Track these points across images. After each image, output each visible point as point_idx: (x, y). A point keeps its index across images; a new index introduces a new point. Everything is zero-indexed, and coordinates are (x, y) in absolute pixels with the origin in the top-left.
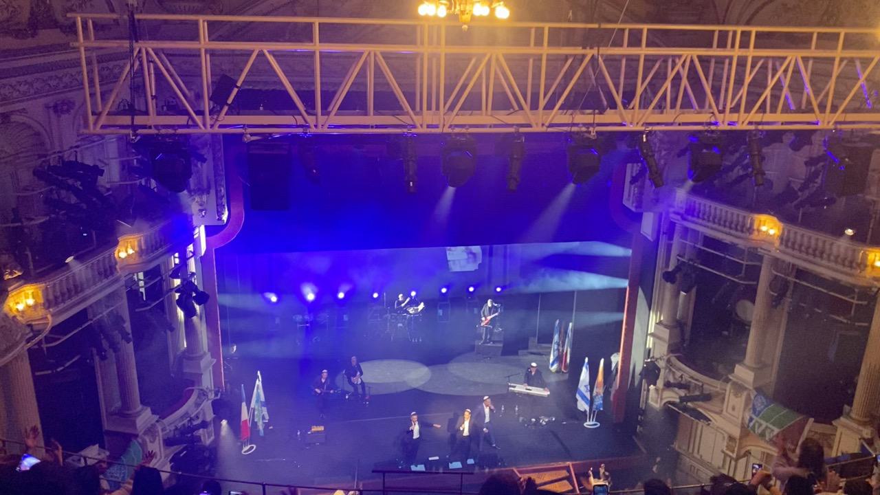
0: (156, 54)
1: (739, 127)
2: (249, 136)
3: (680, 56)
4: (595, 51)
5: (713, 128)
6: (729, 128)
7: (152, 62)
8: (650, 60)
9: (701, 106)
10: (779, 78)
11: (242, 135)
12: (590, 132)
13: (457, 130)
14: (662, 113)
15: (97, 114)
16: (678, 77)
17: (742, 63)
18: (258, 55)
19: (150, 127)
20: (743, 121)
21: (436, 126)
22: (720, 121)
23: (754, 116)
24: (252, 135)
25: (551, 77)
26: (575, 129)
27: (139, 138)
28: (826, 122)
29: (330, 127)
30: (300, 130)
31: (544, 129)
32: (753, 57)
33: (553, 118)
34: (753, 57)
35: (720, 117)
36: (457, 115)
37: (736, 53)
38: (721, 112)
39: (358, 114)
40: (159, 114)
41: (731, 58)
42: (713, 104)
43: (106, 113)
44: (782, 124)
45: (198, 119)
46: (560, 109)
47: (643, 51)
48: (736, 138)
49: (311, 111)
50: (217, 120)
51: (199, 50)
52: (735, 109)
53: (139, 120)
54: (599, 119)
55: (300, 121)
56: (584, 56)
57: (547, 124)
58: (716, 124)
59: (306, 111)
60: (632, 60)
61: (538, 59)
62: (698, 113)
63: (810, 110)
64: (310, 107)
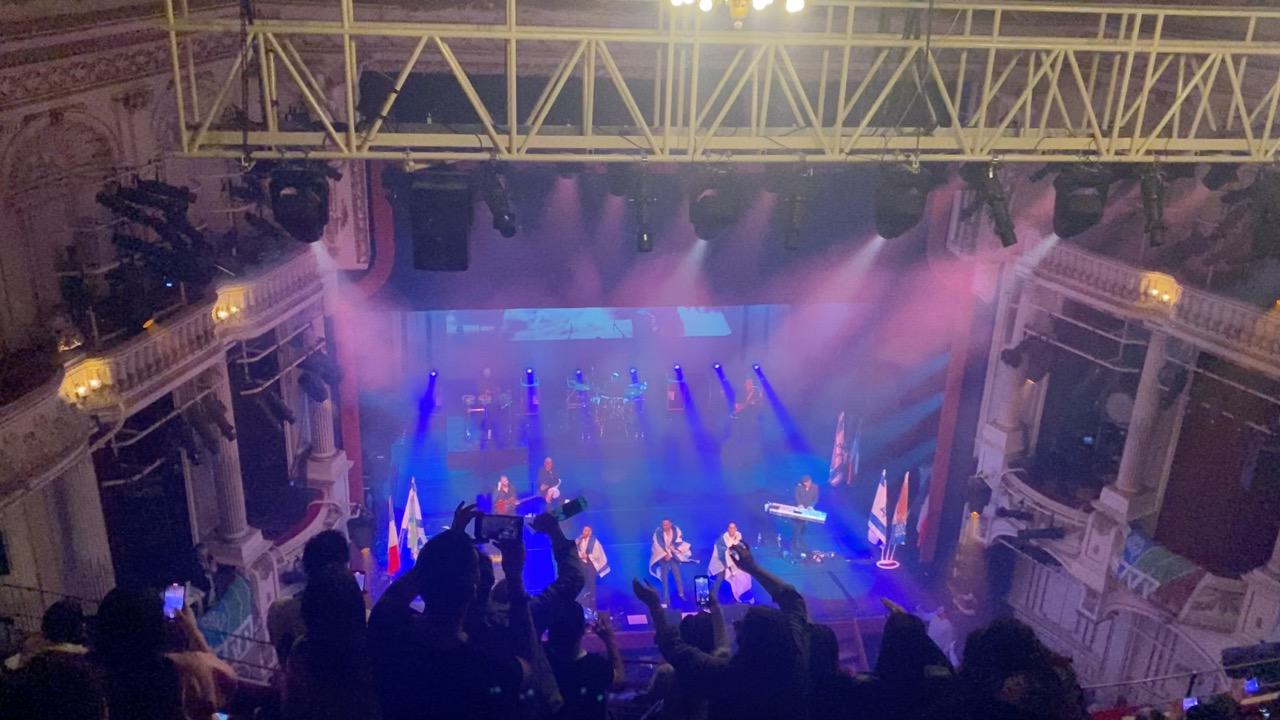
0: (284, 48)
1: (1132, 158)
2: (412, 164)
3: (1048, 52)
4: (922, 43)
5: (1093, 158)
6: (1117, 159)
7: (271, 50)
8: (1003, 57)
9: (1077, 123)
10: (1196, 87)
11: (402, 162)
12: (910, 163)
13: (714, 158)
14: (1017, 135)
15: (194, 128)
16: (1042, 88)
17: (1142, 59)
18: (427, 46)
19: (270, 149)
20: (1138, 149)
21: (684, 152)
22: (1103, 150)
23: (1155, 142)
24: (417, 161)
25: (852, 87)
26: (888, 158)
27: (253, 164)
28: (1262, 153)
29: (529, 151)
30: (485, 156)
31: (842, 157)
32: (1158, 54)
33: (855, 143)
34: (1158, 54)
35: (1103, 143)
36: (715, 135)
37: (1133, 46)
38: (1105, 134)
39: (570, 133)
40: (282, 128)
41: (1124, 56)
42: (1094, 122)
43: (207, 124)
44: (1196, 154)
45: (339, 137)
46: (870, 124)
47: (995, 43)
48: (1125, 172)
49: (501, 126)
50: (366, 139)
51: (342, 36)
52: (1127, 131)
53: (255, 138)
54: (926, 142)
55: (487, 143)
56: (905, 50)
57: (847, 150)
58: (1094, 153)
59: (494, 127)
60: (978, 57)
61: (837, 52)
62: (1071, 135)
63: (1240, 134)
64: (500, 117)
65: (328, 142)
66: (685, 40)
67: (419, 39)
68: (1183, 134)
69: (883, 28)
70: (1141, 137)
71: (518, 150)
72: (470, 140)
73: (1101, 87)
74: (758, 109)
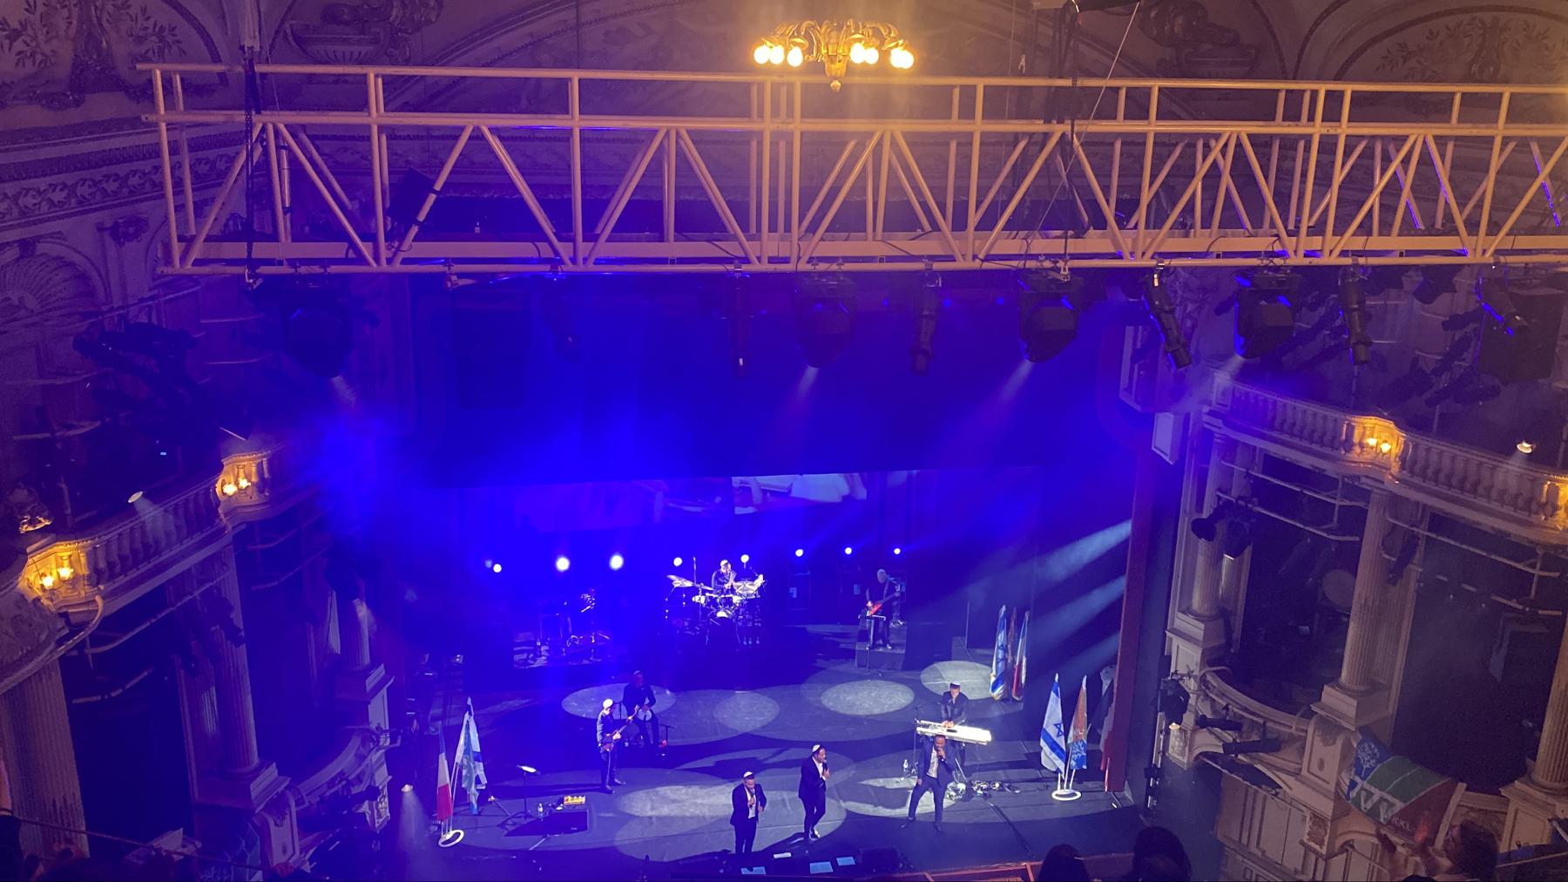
0: (294, 136)
1: (1324, 260)
2: (454, 278)
3: (1217, 136)
4: (1066, 127)
5: (1278, 261)
6: (1307, 261)
8: (1165, 144)
9: (1257, 222)
11: (443, 276)
12: (1058, 270)
13: (822, 267)
14: (1187, 235)
16: (1214, 174)
17: (1328, 145)
19: (280, 263)
20: (1332, 250)
21: (786, 260)
23: (1351, 241)
24: (461, 275)
25: (988, 174)
26: (1031, 264)
27: (259, 282)
28: (1479, 251)
29: (598, 261)
31: (977, 264)
35: (1290, 243)
36: (822, 239)
37: (1318, 129)
38: (1290, 234)
39: (648, 240)
40: (297, 237)
43: (203, 237)
44: (1401, 255)
45: (366, 249)
47: (1152, 127)
48: (1318, 279)
50: (398, 250)
51: (369, 127)
52: (1318, 229)
53: (261, 250)
54: (1075, 246)
55: (547, 252)
56: (1047, 136)
57: (981, 256)
60: (1134, 144)
61: (965, 141)
65: (351, 255)
66: (783, 127)
67: (462, 129)
68: (1386, 228)
69: (1022, 114)
70: (1334, 234)
71: (585, 260)
72: (524, 249)
73: (1284, 176)
74: (875, 208)
